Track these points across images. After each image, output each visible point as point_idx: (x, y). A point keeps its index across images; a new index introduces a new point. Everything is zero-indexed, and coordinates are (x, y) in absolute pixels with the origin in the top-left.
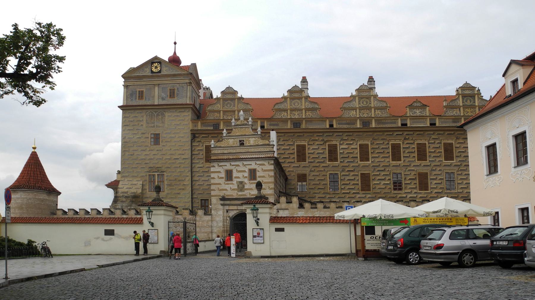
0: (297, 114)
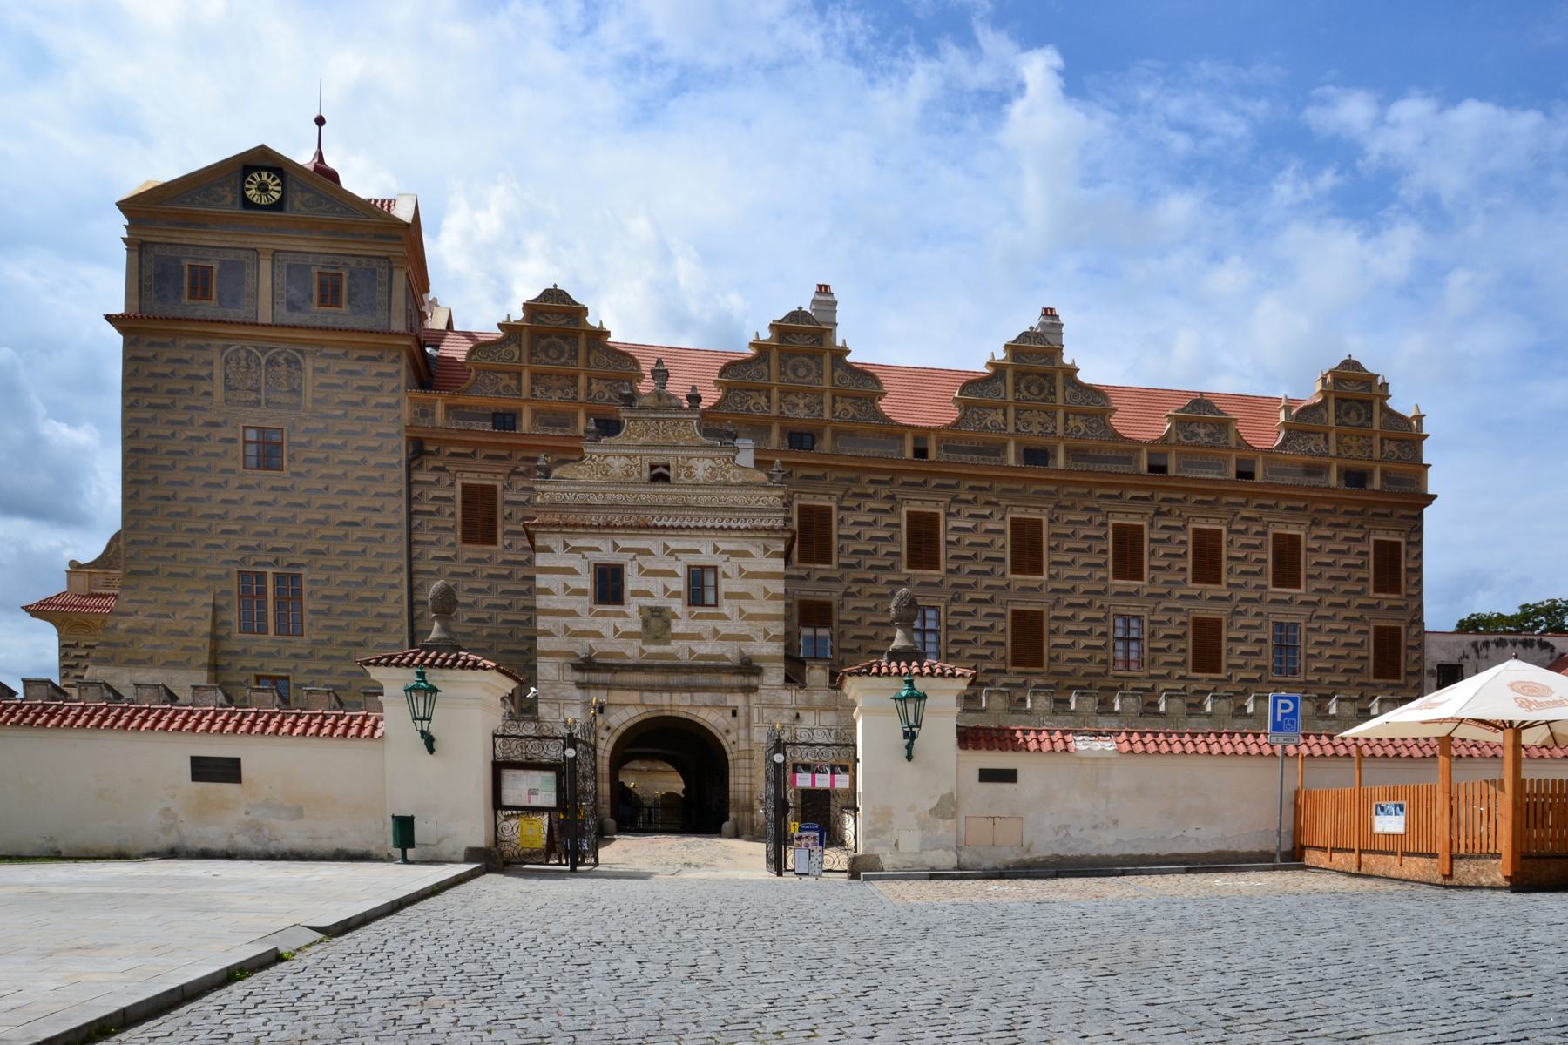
0: (801, 406)
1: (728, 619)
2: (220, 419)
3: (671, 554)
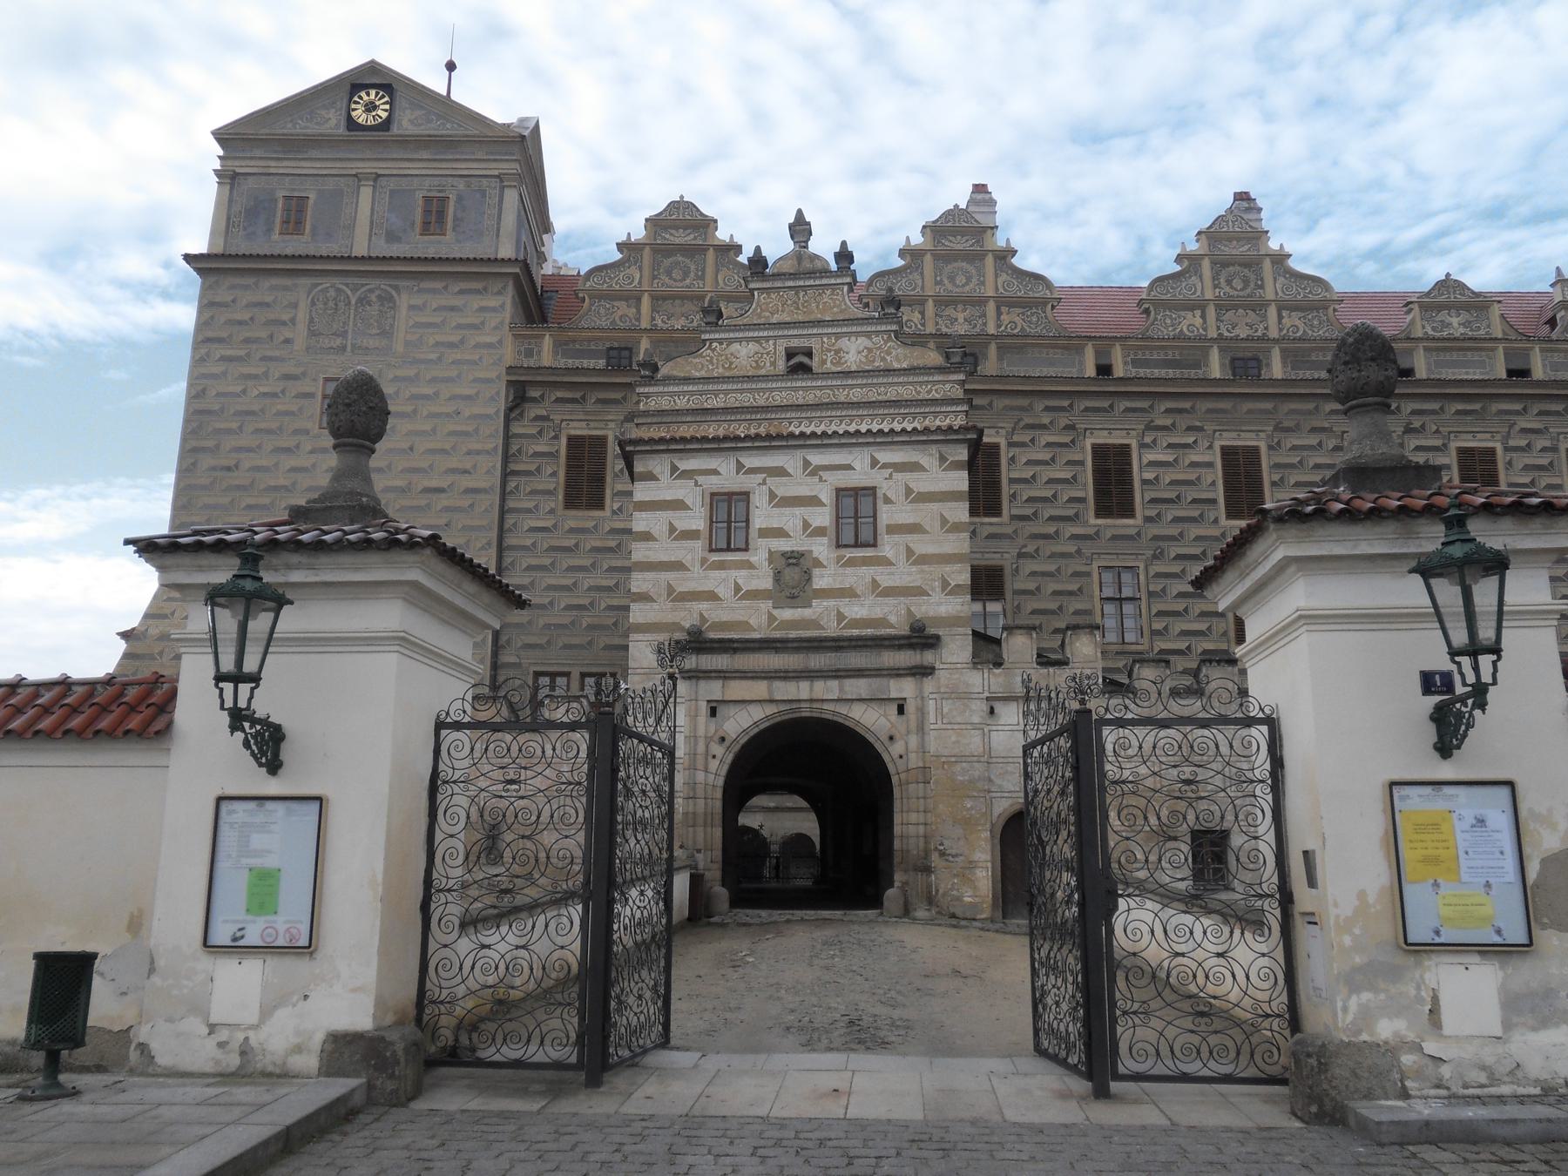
0: (961, 320)
1: (891, 564)
2: (299, 371)
3: (813, 473)
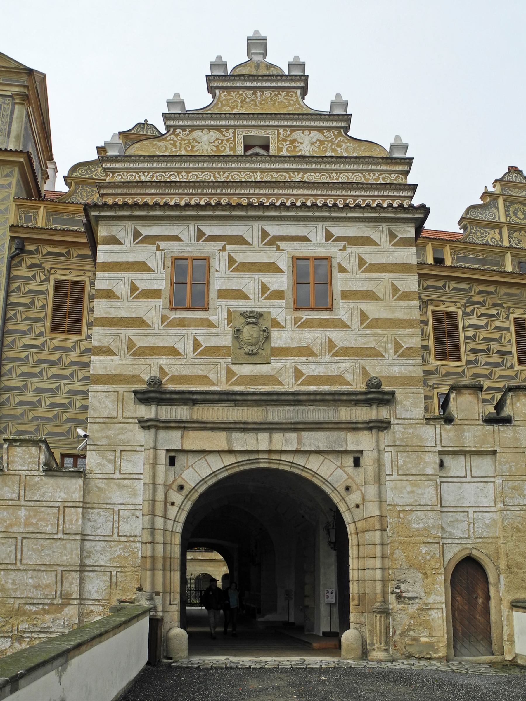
3: (271, 243)
